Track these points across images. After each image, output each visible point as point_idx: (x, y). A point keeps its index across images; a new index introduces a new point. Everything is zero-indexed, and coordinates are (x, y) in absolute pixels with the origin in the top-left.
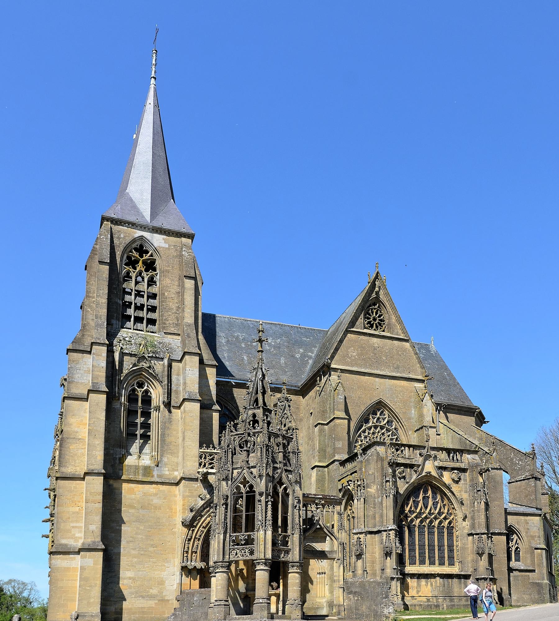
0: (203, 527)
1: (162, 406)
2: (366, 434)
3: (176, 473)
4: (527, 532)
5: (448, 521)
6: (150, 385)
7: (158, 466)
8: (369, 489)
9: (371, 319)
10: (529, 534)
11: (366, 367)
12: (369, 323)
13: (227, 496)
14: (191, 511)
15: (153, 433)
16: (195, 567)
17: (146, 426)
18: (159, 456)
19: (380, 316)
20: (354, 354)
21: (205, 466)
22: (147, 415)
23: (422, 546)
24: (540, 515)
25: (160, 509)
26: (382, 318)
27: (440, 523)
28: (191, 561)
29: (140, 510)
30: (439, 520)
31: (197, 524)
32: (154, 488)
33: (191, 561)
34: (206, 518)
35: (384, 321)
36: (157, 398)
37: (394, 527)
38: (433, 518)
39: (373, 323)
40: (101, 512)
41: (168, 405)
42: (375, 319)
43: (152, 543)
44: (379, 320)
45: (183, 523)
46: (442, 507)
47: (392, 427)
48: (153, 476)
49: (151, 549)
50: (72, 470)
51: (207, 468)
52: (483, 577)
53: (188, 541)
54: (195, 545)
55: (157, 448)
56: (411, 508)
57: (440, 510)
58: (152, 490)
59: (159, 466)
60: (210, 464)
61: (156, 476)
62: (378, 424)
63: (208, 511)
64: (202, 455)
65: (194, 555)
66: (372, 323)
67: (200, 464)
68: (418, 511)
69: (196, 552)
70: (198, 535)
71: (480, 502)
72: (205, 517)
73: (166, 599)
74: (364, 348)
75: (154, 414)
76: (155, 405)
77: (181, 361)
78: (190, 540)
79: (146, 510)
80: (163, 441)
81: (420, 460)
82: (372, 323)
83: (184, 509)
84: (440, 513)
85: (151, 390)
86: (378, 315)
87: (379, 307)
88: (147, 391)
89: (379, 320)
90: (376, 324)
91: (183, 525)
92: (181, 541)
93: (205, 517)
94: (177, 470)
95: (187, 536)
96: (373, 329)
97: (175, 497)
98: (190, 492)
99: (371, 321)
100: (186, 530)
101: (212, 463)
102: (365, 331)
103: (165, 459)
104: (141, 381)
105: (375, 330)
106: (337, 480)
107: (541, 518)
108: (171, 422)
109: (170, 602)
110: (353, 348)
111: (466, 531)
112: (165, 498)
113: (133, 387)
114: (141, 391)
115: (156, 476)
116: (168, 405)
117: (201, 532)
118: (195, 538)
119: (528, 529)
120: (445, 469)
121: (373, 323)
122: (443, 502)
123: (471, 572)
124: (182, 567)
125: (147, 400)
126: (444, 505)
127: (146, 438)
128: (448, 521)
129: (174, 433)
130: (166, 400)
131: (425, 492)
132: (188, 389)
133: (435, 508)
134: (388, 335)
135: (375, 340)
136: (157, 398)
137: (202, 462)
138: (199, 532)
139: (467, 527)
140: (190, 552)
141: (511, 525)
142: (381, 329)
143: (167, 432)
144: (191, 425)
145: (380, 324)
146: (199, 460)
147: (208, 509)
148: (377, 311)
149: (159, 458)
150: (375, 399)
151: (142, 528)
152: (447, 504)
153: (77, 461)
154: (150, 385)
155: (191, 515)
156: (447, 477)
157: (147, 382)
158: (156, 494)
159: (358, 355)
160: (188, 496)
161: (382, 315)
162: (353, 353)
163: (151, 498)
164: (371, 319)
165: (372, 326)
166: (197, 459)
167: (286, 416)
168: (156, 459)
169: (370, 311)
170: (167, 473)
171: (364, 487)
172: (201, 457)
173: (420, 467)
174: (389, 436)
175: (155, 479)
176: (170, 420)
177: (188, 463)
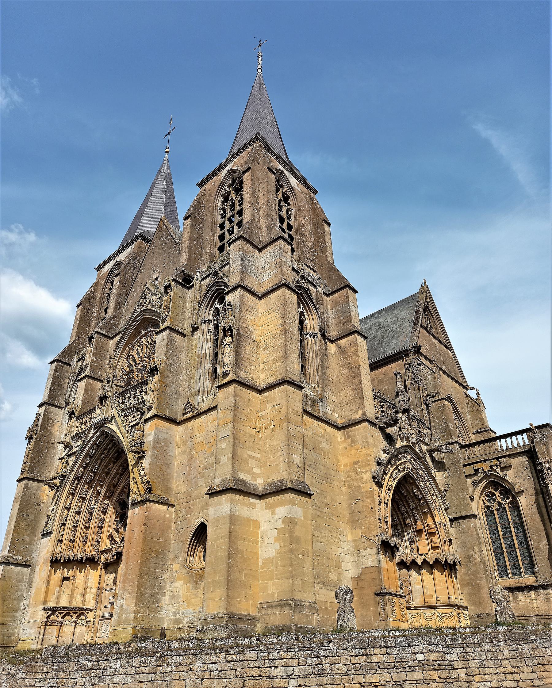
29: (312, 453)
32: (322, 428)
45: (374, 478)
48: (319, 412)
49: (326, 510)
50: (248, 376)
61: (321, 412)
79: (317, 455)
80: (323, 373)
91: (375, 482)
106: (462, 463)
115: (321, 412)
147: (389, 466)
158: (323, 436)
163: (321, 439)
170: (330, 412)
175: (321, 415)
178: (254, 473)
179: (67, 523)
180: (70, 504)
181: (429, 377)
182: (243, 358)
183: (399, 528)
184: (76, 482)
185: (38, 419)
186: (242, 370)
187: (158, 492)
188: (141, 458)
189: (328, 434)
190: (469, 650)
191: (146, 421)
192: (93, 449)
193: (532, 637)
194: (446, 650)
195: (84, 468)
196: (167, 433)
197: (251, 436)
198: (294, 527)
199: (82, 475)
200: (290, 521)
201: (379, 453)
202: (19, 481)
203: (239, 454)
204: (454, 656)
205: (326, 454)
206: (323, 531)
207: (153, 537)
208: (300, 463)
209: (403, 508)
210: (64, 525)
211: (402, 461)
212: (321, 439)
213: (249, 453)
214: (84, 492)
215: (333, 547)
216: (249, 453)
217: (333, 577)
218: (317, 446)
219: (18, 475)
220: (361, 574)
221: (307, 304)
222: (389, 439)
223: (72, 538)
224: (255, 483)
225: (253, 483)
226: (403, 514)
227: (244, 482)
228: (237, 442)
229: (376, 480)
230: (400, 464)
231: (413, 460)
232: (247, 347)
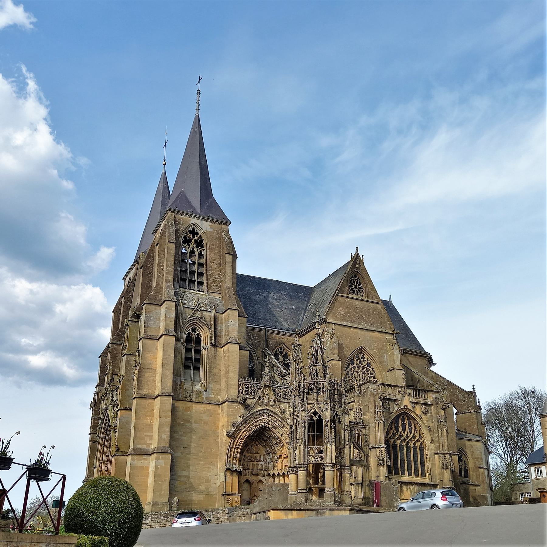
0: (241, 439)
1: (210, 347)
2: (352, 372)
3: (219, 397)
4: (472, 455)
5: (420, 442)
6: (200, 329)
7: (206, 391)
8: (364, 416)
9: (353, 287)
10: (474, 456)
11: (351, 323)
12: (352, 289)
13: (305, 421)
14: (233, 426)
15: (203, 366)
16: (236, 469)
17: (198, 360)
18: (207, 383)
19: (359, 285)
20: (342, 312)
21: (242, 393)
22: (198, 352)
23: (402, 461)
24: (482, 441)
25: (207, 423)
26: (361, 286)
27: (414, 444)
28: (233, 465)
30: (413, 442)
31: (237, 437)
33: (233, 465)
34: (243, 432)
35: (362, 289)
36: (206, 340)
37: (384, 446)
38: (410, 440)
39: (355, 290)
40: (170, 425)
41: (215, 345)
42: (356, 287)
43: (202, 449)
44: (359, 288)
45: (227, 435)
46: (416, 432)
47: (370, 367)
48: (203, 398)
49: (201, 454)
51: (244, 394)
52: (448, 486)
53: (230, 449)
54: (235, 452)
55: (205, 377)
56: (394, 432)
57: (414, 434)
58: (202, 409)
59: (207, 391)
60: (246, 391)
61: (205, 398)
62: (360, 365)
63: (245, 427)
64: (241, 384)
65: (234, 460)
66: (354, 290)
67: (239, 391)
68: (399, 433)
69: (236, 458)
70: (237, 445)
71: (443, 430)
72: (243, 431)
73: (211, 494)
74: (349, 308)
75: (203, 352)
76: (204, 345)
77: (223, 313)
78: (231, 448)
79: (198, 425)
80: (211, 372)
81: (399, 396)
82: (354, 290)
83: (228, 425)
84: (414, 437)
85: (201, 333)
86: (358, 284)
87: (358, 278)
88: (198, 335)
89: (359, 288)
90: (357, 291)
92: (226, 449)
93: (243, 431)
94: (220, 395)
95: (230, 446)
96: (355, 294)
97: (218, 415)
98: (232, 412)
99: (353, 289)
100: (229, 440)
101: (248, 391)
102: (350, 296)
103: (211, 386)
104: (194, 327)
105: (356, 295)
107: (482, 444)
108: (216, 358)
109: (214, 496)
110: (341, 308)
111: (433, 452)
112: (211, 416)
113: (189, 331)
114: (194, 335)
115: (205, 398)
116: (215, 345)
117: (239, 443)
118: (236, 447)
119: (473, 452)
120: (417, 403)
121: (355, 290)
122: (416, 429)
123: (438, 483)
124: (226, 469)
125: (198, 341)
126: (417, 431)
127: (197, 369)
128: (420, 442)
129: (218, 366)
130: (213, 342)
131: (403, 421)
132: (231, 335)
133: (411, 433)
134: (366, 299)
135: (357, 303)
136: (206, 340)
137: (240, 389)
138: (238, 443)
139: (433, 448)
140: (232, 457)
141: (460, 448)
142: (360, 294)
143: (213, 366)
144: (233, 362)
145: (360, 291)
146: (239, 388)
148: (357, 281)
149: (207, 385)
150: (358, 347)
151: (195, 438)
152: (419, 430)
153: (150, 386)
154: (200, 329)
155: (233, 429)
156: (418, 410)
157: (199, 328)
158: (204, 413)
159: (345, 313)
160: (231, 415)
161: (361, 284)
162: (341, 311)
163: (201, 415)
164: (353, 287)
165: (354, 292)
166: (237, 387)
167: (298, 357)
168: (205, 386)
169: (352, 281)
170: (213, 396)
171: (361, 415)
172: (239, 385)
173: (400, 402)
174: (368, 374)
175: (205, 400)
176: (215, 357)
177: (231, 390)
178: (148, 443)
179: (103, 462)
180: (103, 452)
181: (328, 342)
182: (143, 382)
184: (104, 440)
185: (95, 396)
186: (141, 389)
187: (123, 449)
188: (116, 432)
189: (210, 410)
190: (153, 520)
191: (117, 411)
192: (107, 423)
193: (172, 515)
194: (146, 520)
195: (106, 433)
196: (128, 417)
197: (147, 425)
198: (157, 470)
199: (106, 436)
200: (156, 467)
201: (236, 418)
202: (90, 434)
203: (138, 435)
204: (148, 522)
205: (205, 423)
206: (197, 466)
207: (120, 473)
208: (166, 438)
209: (270, 444)
210: (102, 463)
211: (260, 419)
212: (201, 415)
213: (145, 434)
214: (109, 444)
215: (204, 473)
216: (145, 434)
217: (202, 488)
218: (198, 419)
219: (89, 431)
220: (220, 485)
221: (202, 327)
222: (247, 407)
223: (106, 470)
224: (148, 448)
225: (147, 448)
226: (271, 447)
227: (141, 449)
228: (136, 430)
229: (228, 436)
230: (257, 421)
231: (270, 416)
232: (146, 375)
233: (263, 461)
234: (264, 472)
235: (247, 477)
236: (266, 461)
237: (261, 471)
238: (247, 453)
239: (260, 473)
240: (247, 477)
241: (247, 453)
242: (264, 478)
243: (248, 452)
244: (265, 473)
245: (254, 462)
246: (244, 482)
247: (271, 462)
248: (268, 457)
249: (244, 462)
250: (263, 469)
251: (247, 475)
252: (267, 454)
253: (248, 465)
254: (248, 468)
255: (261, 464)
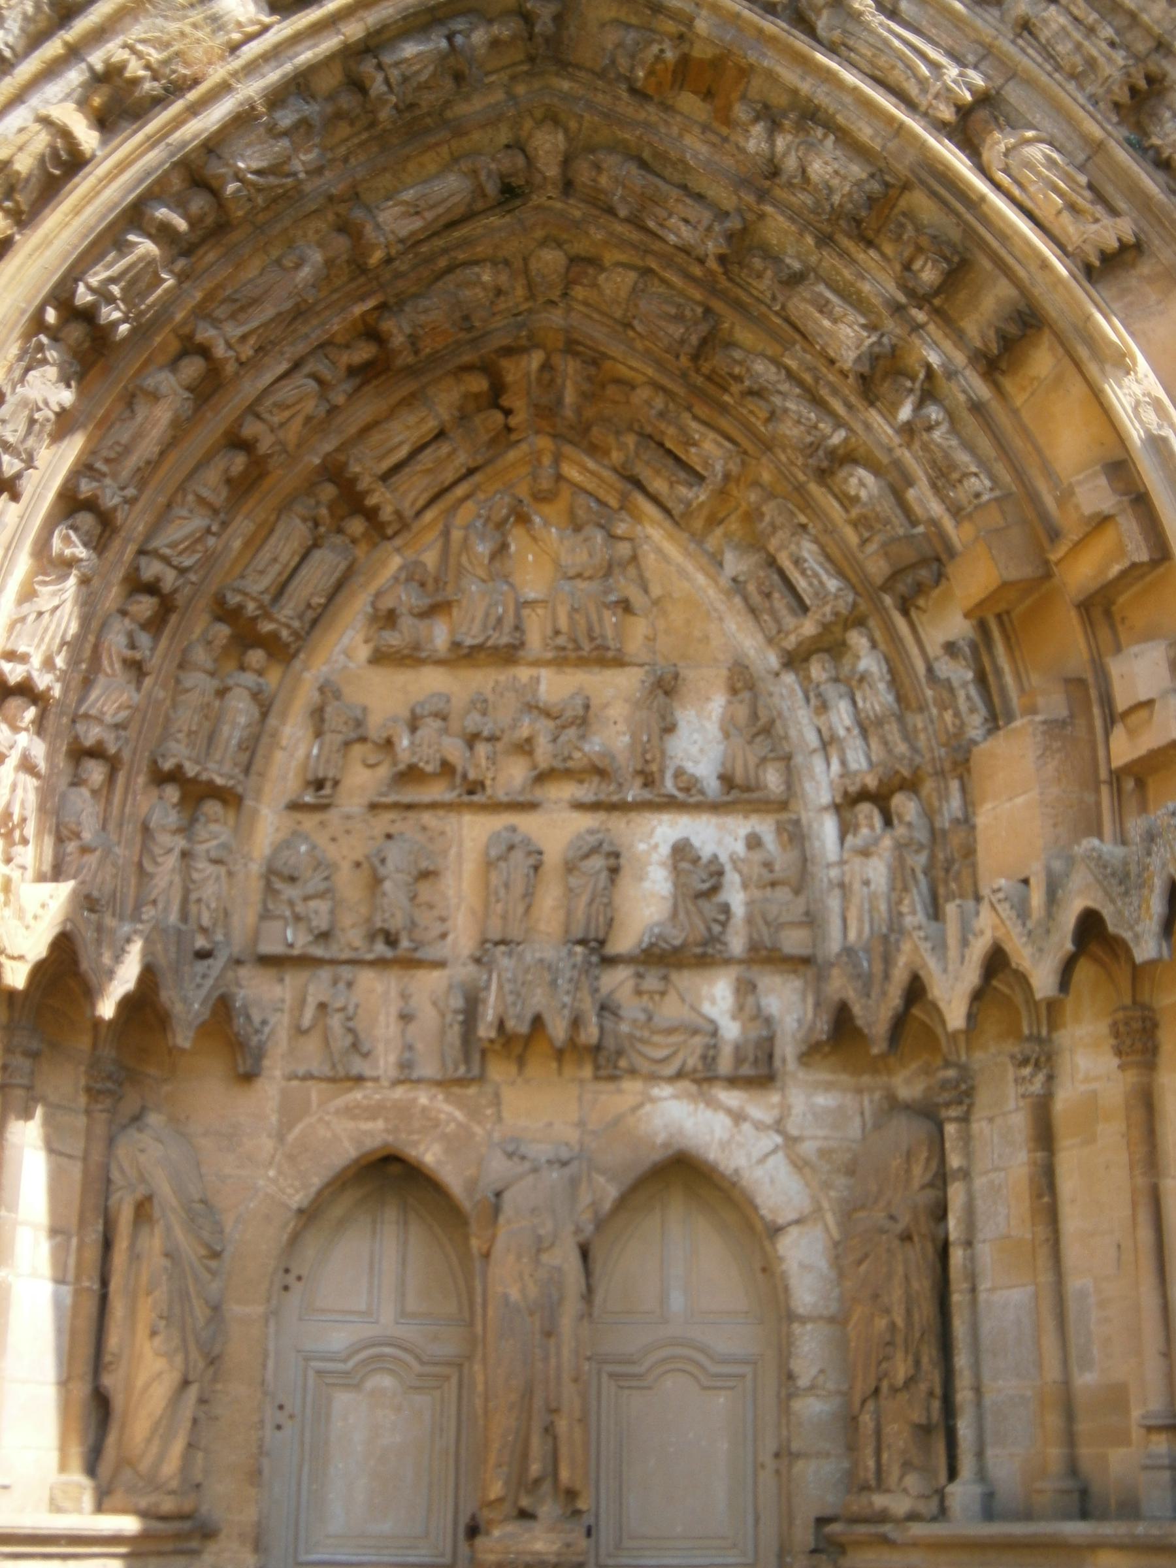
183: (869, 663)
233: (727, 780)
234: (745, 989)
235: (372, 1112)
236: (773, 779)
237: (684, 979)
238: (379, 658)
239: (671, 1010)
240: (372, 1112)
241: (379, 658)
242: (760, 1106)
243: (393, 639)
244: (768, 1021)
245: (527, 823)
246: (298, 1199)
247: (880, 798)
248: (823, 707)
249: (309, 822)
250: (712, 940)
251: (386, 1062)
252: (794, 660)
253: (395, 855)
254: (391, 940)
255: (682, 852)
